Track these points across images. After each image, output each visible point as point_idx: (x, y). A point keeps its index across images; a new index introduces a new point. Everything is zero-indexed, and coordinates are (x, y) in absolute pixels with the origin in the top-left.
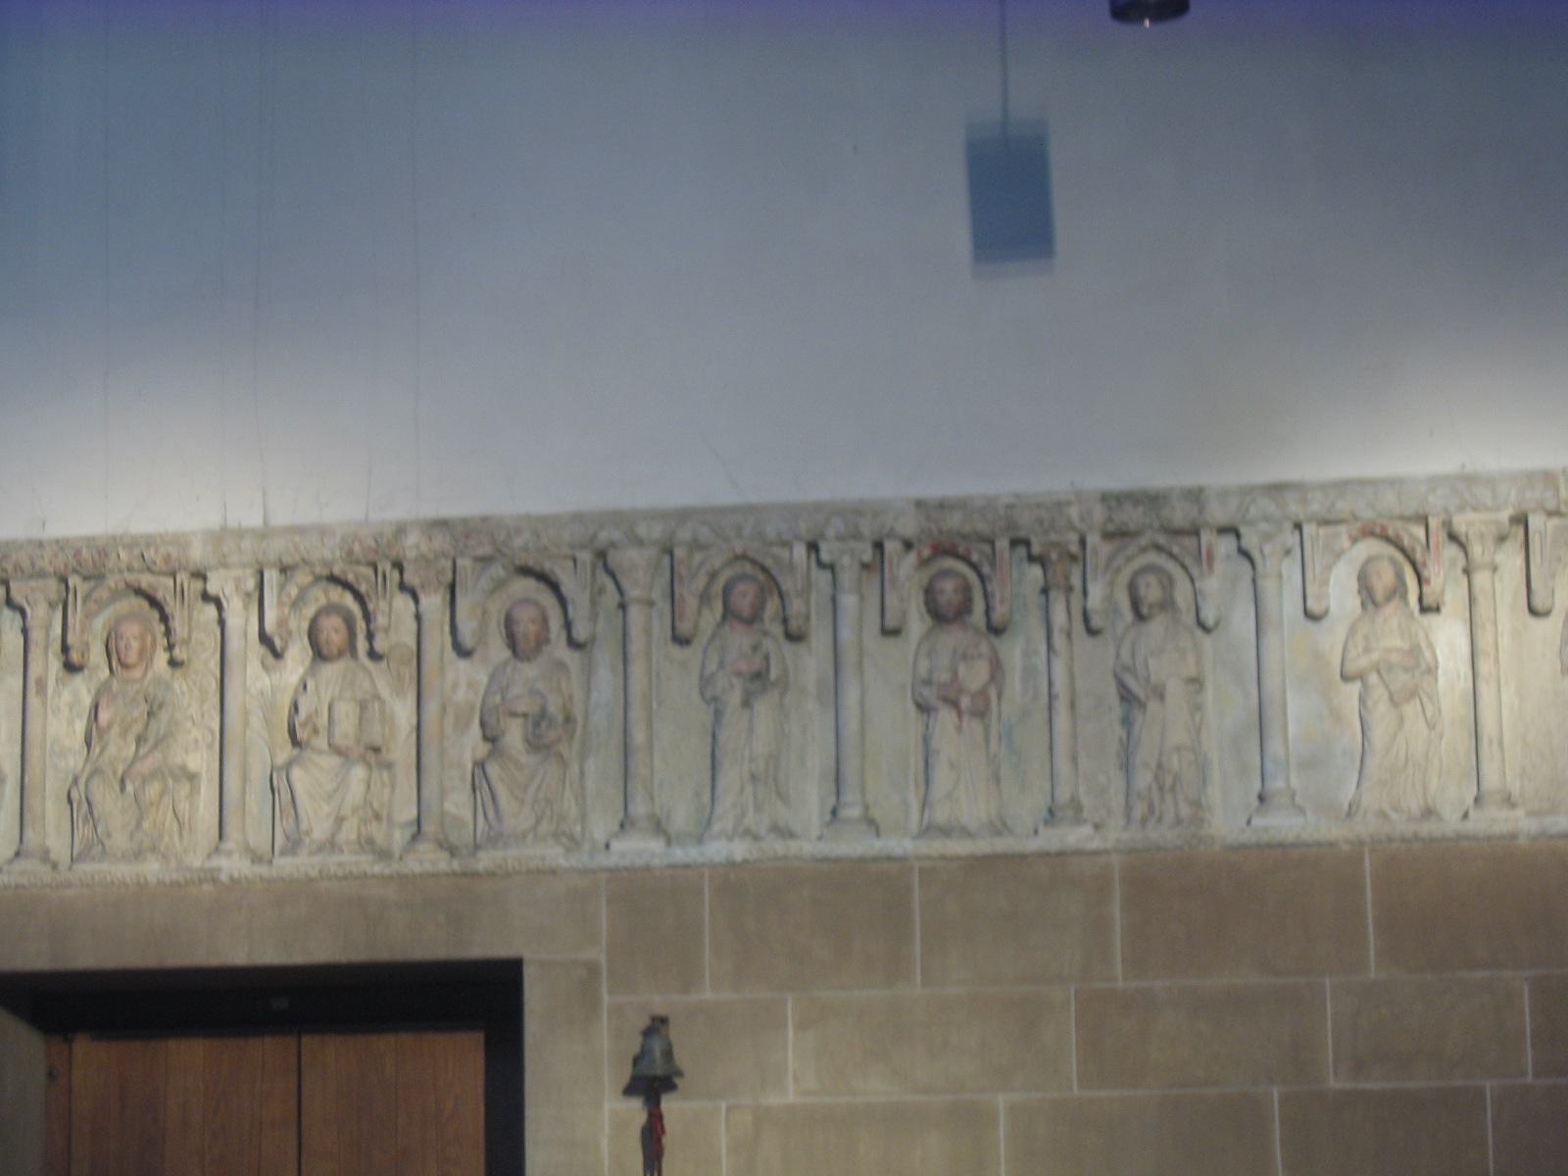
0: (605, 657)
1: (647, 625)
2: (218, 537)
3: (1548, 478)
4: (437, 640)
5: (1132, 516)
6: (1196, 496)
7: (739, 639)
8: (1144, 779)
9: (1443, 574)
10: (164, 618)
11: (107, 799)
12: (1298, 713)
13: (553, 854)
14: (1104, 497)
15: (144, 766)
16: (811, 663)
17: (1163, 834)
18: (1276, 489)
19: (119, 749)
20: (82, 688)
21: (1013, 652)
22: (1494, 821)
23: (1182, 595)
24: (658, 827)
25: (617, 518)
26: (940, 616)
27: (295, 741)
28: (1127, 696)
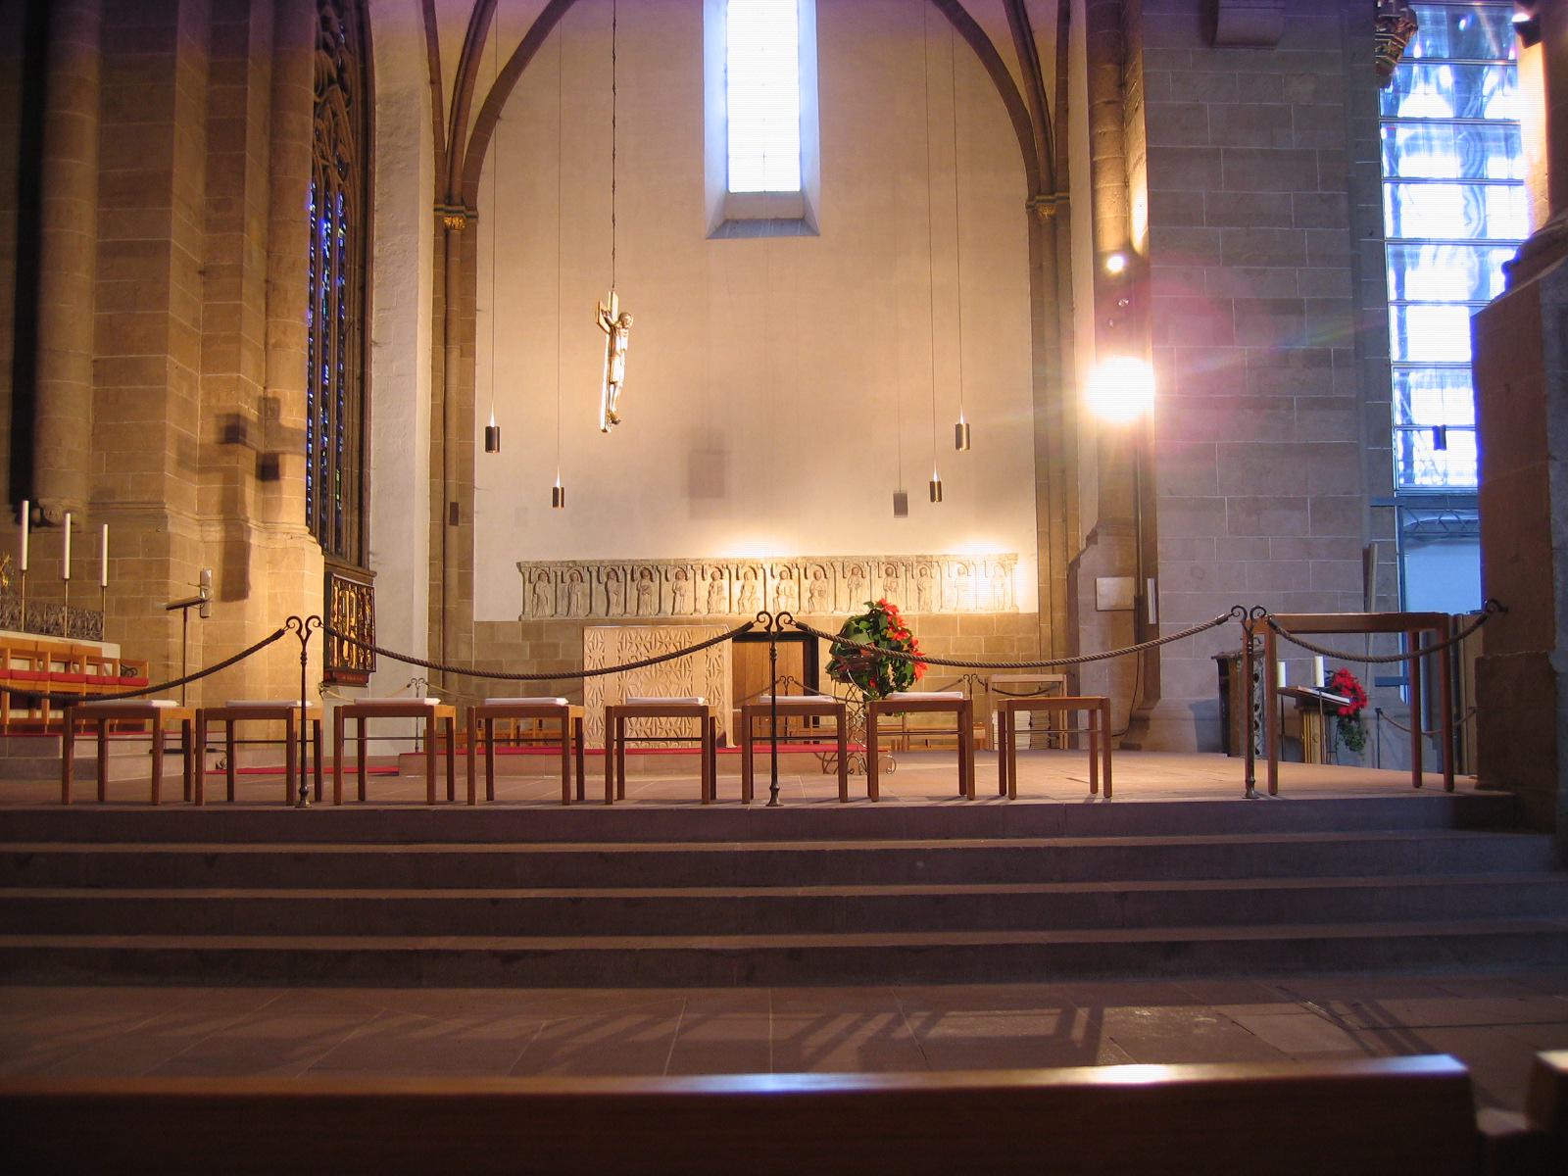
0: (832, 581)
1: (839, 575)
2: (766, 559)
3: (989, 555)
4: (802, 576)
5: (921, 559)
6: (931, 556)
7: (855, 578)
8: (922, 603)
9: (972, 569)
10: (756, 574)
11: (746, 603)
12: (947, 592)
13: (824, 614)
14: (917, 556)
15: (753, 597)
16: (866, 582)
17: (926, 612)
18: (945, 556)
19: (747, 593)
20: (741, 581)
21: (900, 581)
22: (979, 612)
23: (929, 572)
24: (841, 610)
25: (835, 557)
26: (888, 575)
27: (778, 592)
28: (919, 589)
